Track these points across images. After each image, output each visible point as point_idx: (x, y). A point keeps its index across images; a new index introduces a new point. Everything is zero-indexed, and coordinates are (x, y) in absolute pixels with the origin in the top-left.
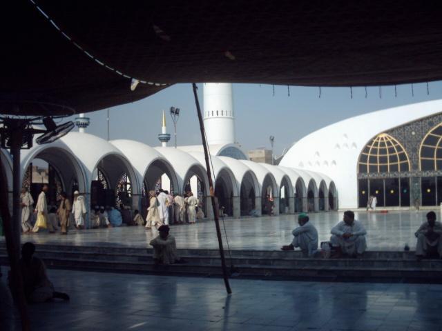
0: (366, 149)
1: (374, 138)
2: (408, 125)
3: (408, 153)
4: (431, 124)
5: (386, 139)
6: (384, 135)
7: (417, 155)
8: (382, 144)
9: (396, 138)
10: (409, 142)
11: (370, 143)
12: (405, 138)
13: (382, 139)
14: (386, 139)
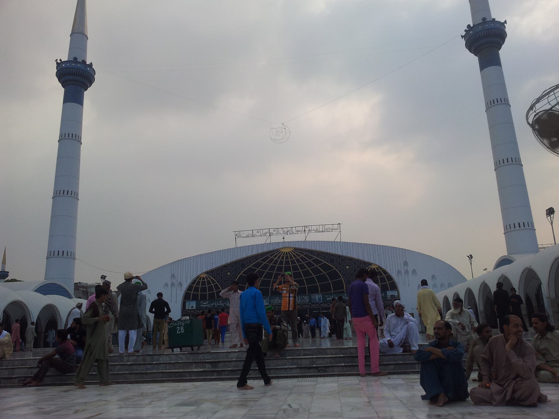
0: (190, 288)
1: (197, 279)
2: (225, 266)
4: (243, 266)
6: (204, 276)
8: (203, 283)
11: (193, 282)
13: (204, 278)
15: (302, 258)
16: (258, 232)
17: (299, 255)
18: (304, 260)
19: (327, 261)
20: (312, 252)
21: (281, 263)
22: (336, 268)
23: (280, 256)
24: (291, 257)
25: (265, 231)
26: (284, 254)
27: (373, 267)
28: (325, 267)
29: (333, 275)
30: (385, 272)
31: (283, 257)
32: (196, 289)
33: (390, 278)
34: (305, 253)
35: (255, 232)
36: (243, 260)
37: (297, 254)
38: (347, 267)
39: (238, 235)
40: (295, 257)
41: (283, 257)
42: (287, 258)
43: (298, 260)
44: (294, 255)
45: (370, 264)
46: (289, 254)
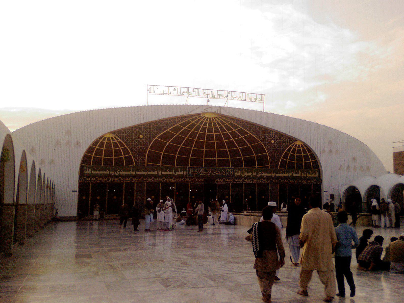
0: (90, 150)
1: (100, 138)
2: (137, 127)
3: (134, 157)
5: (113, 140)
6: (110, 136)
7: (144, 160)
8: (109, 145)
9: (123, 140)
10: (136, 145)
11: (95, 143)
12: (132, 140)
13: (109, 138)
14: (113, 140)
15: (226, 126)
16: (174, 90)
17: (223, 123)
18: (229, 129)
19: (252, 133)
20: (238, 121)
21: (204, 130)
22: (262, 141)
23: (202, 122)
24: (215, 125)
25: (183, 90)
26: (207, 120)
27: (298, 143)
28: (251, 139)
29: (259, 149)
30: (309, 150)
31: (206, 123)
32: (99, 152)
33: (313, 156)
34: (230, 122)
35: (191, 90)
36: (159, 122)
37: (221, 121)
38: (273, 142)
39: (150, 89)
40: (219, 125)
41: (206, 123)
42: (210, 125)
43: (221, 128)
44: (218, 123)
45: (296, 140)
46: (213, 120)
